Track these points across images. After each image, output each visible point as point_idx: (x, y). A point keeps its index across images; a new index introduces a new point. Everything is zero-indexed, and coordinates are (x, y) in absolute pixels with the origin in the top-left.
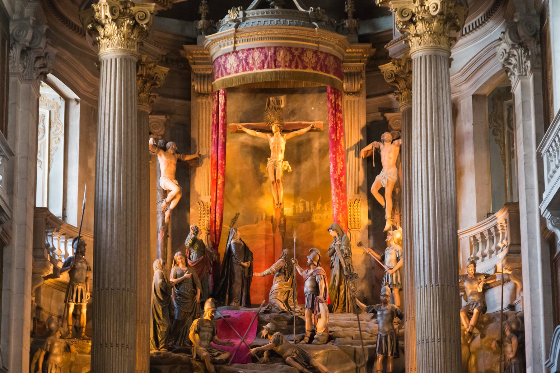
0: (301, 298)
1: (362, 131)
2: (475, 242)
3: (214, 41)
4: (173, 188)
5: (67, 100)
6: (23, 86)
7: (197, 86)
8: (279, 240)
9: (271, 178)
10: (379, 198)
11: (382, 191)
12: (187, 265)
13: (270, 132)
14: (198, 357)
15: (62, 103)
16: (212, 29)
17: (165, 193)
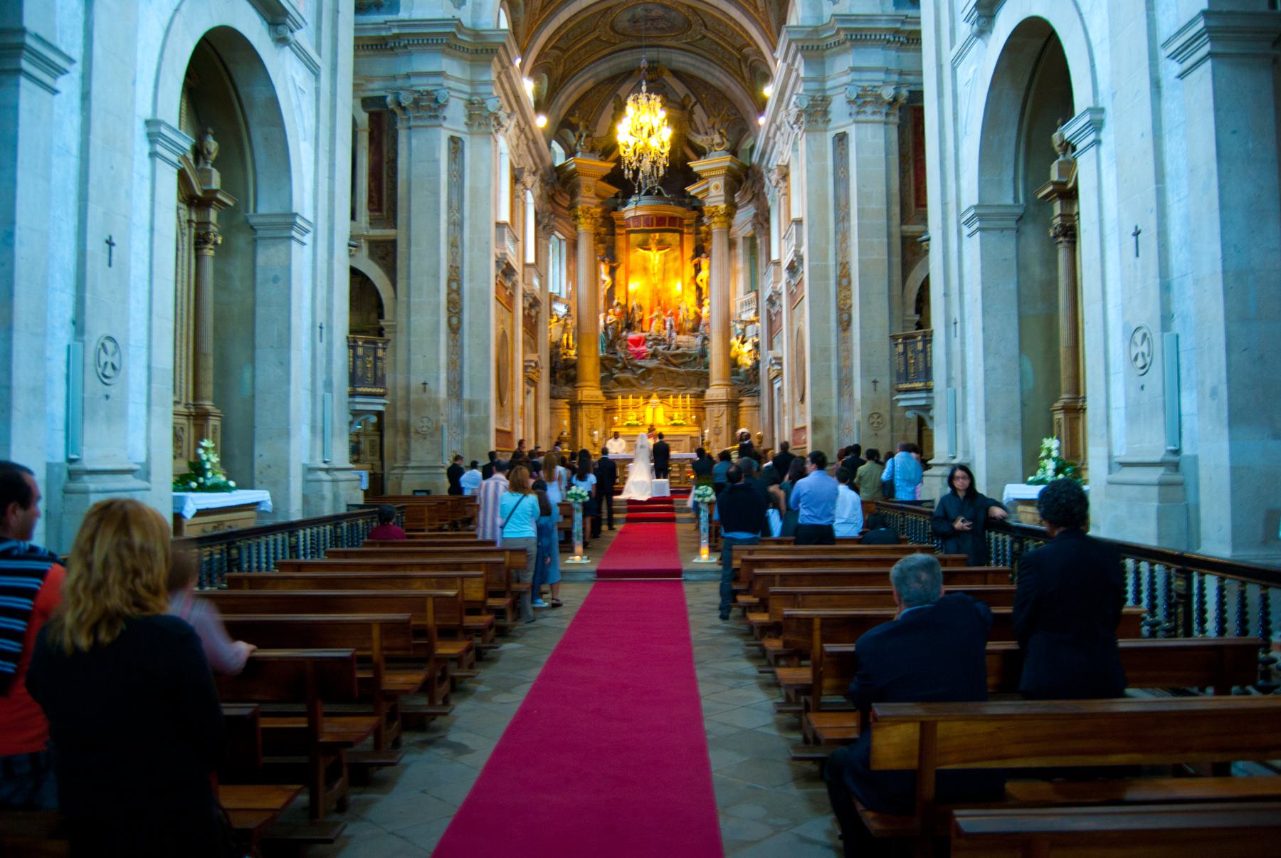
0: (665, 329)
1: (694, 251)
2: (742, 305)
3: (626, 211)
4: (608, 280)
5: (560, 240)
6: (544, 242)
7: (618, 231)
8: (656, 303)
9: (652, 272)
10: (700, 284)
11: (701, 280)
12: (615, 315)
13: (649, 249)
14: (621, 358)
15: (558, 241)
16: (625, 205)
17: (604, 281)
